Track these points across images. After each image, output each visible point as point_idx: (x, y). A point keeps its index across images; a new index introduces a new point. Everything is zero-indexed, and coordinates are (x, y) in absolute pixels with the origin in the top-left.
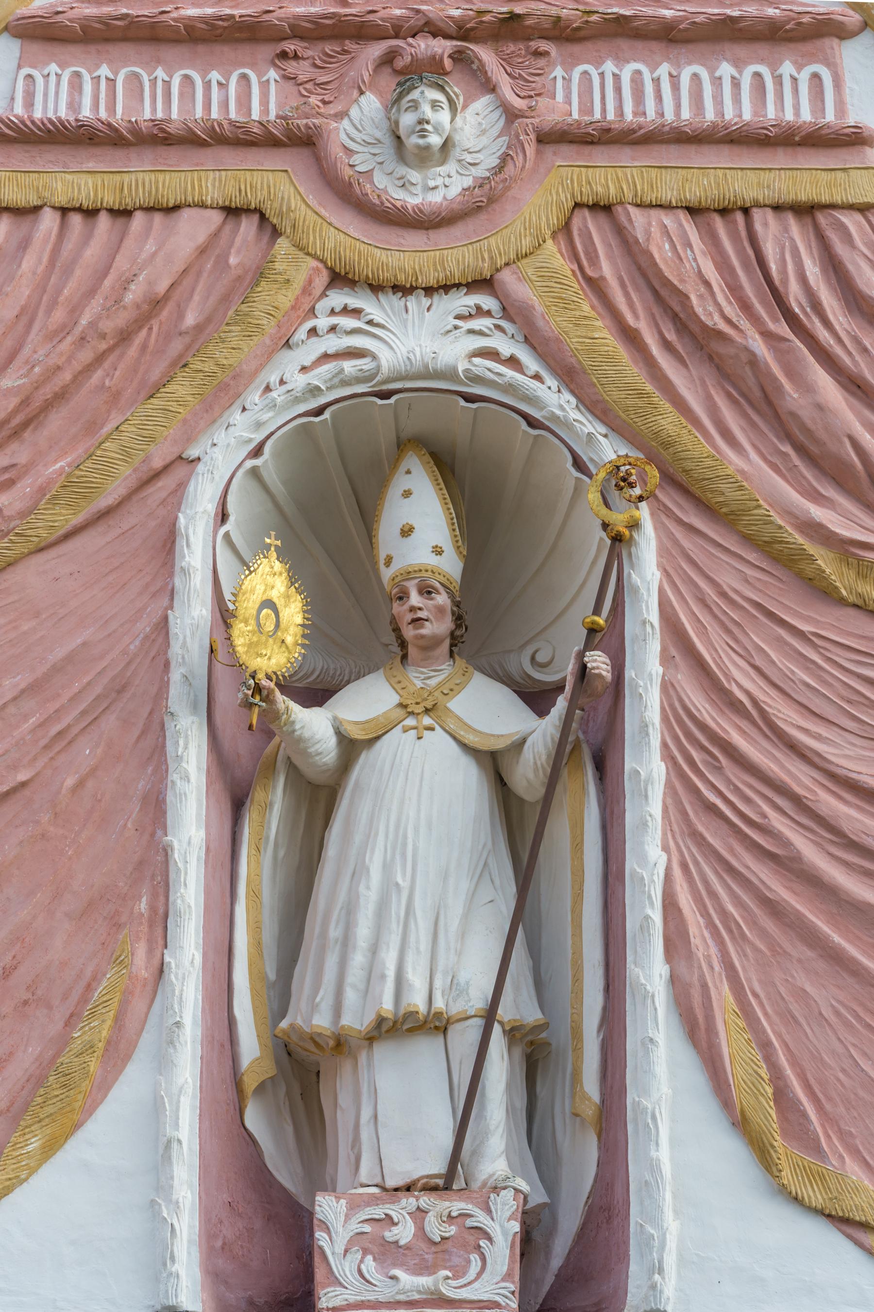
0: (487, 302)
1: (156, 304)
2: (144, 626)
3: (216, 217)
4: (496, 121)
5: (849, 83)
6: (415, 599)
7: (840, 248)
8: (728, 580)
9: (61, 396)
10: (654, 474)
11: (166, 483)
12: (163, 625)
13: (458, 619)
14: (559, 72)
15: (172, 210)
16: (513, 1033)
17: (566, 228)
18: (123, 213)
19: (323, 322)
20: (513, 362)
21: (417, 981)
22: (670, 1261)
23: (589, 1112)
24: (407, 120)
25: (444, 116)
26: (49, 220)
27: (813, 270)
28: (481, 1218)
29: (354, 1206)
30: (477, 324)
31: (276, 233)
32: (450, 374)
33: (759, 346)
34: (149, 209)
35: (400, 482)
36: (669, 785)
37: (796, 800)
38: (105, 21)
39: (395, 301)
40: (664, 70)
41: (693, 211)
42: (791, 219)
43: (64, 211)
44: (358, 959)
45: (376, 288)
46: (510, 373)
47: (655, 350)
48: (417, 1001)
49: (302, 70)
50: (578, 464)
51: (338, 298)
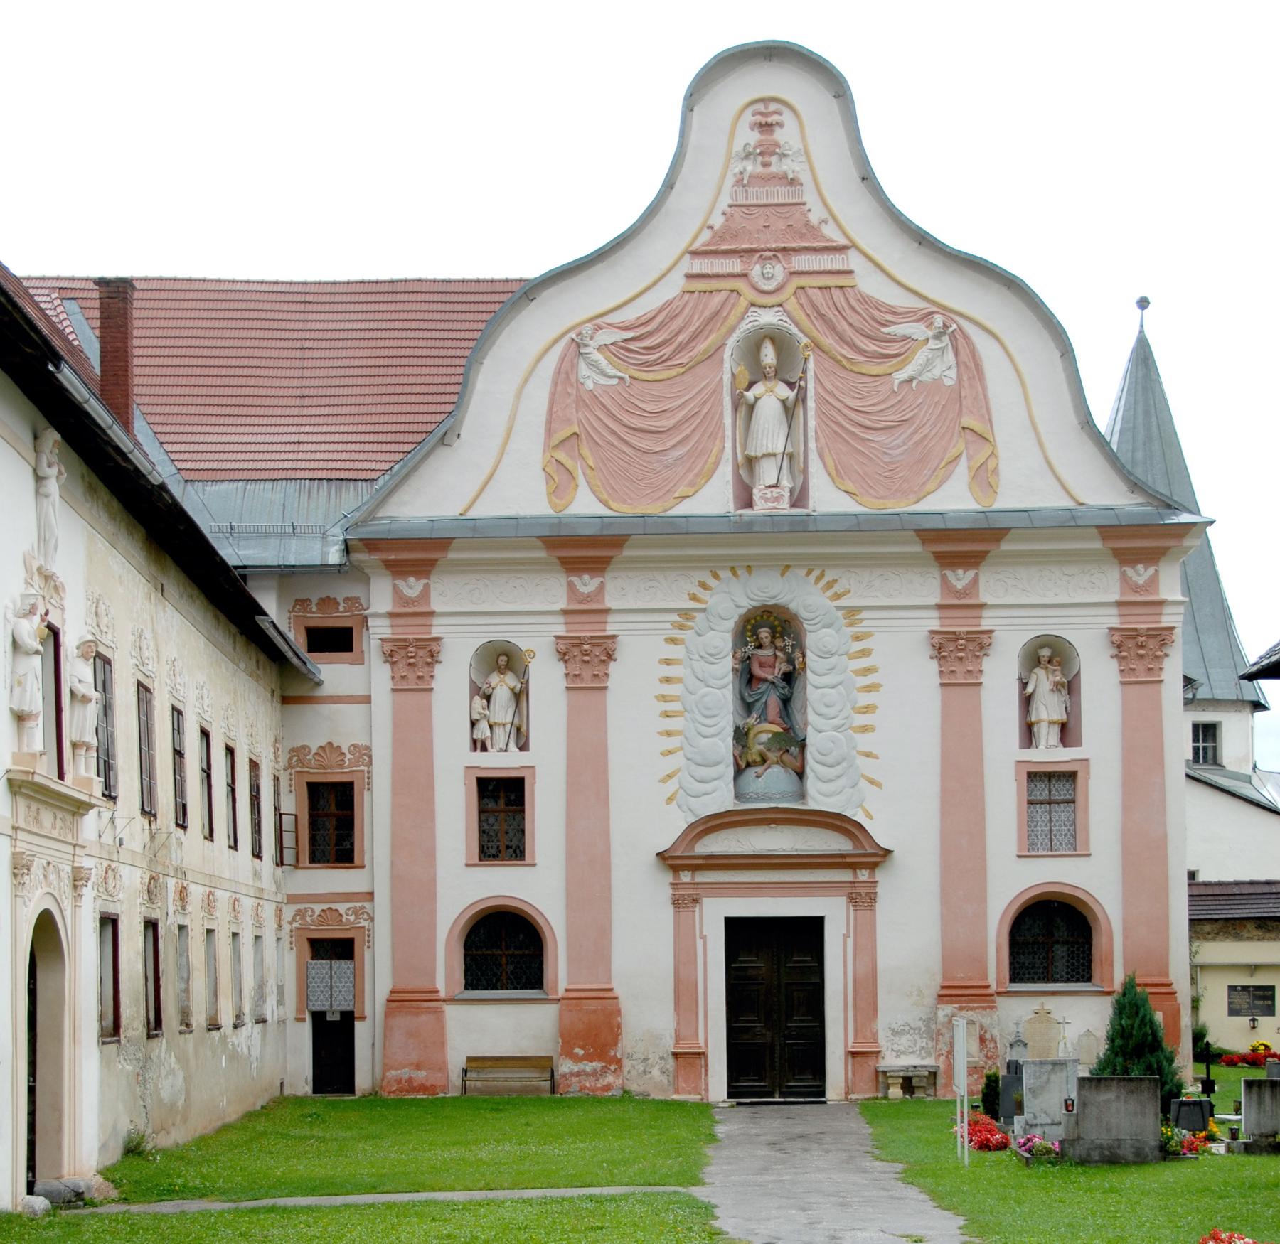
0: (780, 309)
3: (729, 292)
4: (782, 269)
6: (768, 369)
7: (848, 296)
8: (826, 366)
11: (719, 351)
12: (722, 378)
13: (776, 372)
14: (793, 258)
15: (720, 291)
17: (795, 292)
18: (711, 292)
19: (749, 314)
20: (786, 322)
21: (770, 445)
24: (765, 271)
25: (772, 271)
28: (782, 493)
30: (780, 314)
31: (740, 295)
32: (774, 325)
34: (716, 291)
36: (816, 410)
37: (839, 411)
39: (763, 309)
40: (814, 257)
41: (820, 288)
42: (838, 289)
43: (700, 292)
45: (760, 307)
46: (785, 324)
47: (813, 319)
48: (770, 451)
49: (744, 259)
51: (753, 309)
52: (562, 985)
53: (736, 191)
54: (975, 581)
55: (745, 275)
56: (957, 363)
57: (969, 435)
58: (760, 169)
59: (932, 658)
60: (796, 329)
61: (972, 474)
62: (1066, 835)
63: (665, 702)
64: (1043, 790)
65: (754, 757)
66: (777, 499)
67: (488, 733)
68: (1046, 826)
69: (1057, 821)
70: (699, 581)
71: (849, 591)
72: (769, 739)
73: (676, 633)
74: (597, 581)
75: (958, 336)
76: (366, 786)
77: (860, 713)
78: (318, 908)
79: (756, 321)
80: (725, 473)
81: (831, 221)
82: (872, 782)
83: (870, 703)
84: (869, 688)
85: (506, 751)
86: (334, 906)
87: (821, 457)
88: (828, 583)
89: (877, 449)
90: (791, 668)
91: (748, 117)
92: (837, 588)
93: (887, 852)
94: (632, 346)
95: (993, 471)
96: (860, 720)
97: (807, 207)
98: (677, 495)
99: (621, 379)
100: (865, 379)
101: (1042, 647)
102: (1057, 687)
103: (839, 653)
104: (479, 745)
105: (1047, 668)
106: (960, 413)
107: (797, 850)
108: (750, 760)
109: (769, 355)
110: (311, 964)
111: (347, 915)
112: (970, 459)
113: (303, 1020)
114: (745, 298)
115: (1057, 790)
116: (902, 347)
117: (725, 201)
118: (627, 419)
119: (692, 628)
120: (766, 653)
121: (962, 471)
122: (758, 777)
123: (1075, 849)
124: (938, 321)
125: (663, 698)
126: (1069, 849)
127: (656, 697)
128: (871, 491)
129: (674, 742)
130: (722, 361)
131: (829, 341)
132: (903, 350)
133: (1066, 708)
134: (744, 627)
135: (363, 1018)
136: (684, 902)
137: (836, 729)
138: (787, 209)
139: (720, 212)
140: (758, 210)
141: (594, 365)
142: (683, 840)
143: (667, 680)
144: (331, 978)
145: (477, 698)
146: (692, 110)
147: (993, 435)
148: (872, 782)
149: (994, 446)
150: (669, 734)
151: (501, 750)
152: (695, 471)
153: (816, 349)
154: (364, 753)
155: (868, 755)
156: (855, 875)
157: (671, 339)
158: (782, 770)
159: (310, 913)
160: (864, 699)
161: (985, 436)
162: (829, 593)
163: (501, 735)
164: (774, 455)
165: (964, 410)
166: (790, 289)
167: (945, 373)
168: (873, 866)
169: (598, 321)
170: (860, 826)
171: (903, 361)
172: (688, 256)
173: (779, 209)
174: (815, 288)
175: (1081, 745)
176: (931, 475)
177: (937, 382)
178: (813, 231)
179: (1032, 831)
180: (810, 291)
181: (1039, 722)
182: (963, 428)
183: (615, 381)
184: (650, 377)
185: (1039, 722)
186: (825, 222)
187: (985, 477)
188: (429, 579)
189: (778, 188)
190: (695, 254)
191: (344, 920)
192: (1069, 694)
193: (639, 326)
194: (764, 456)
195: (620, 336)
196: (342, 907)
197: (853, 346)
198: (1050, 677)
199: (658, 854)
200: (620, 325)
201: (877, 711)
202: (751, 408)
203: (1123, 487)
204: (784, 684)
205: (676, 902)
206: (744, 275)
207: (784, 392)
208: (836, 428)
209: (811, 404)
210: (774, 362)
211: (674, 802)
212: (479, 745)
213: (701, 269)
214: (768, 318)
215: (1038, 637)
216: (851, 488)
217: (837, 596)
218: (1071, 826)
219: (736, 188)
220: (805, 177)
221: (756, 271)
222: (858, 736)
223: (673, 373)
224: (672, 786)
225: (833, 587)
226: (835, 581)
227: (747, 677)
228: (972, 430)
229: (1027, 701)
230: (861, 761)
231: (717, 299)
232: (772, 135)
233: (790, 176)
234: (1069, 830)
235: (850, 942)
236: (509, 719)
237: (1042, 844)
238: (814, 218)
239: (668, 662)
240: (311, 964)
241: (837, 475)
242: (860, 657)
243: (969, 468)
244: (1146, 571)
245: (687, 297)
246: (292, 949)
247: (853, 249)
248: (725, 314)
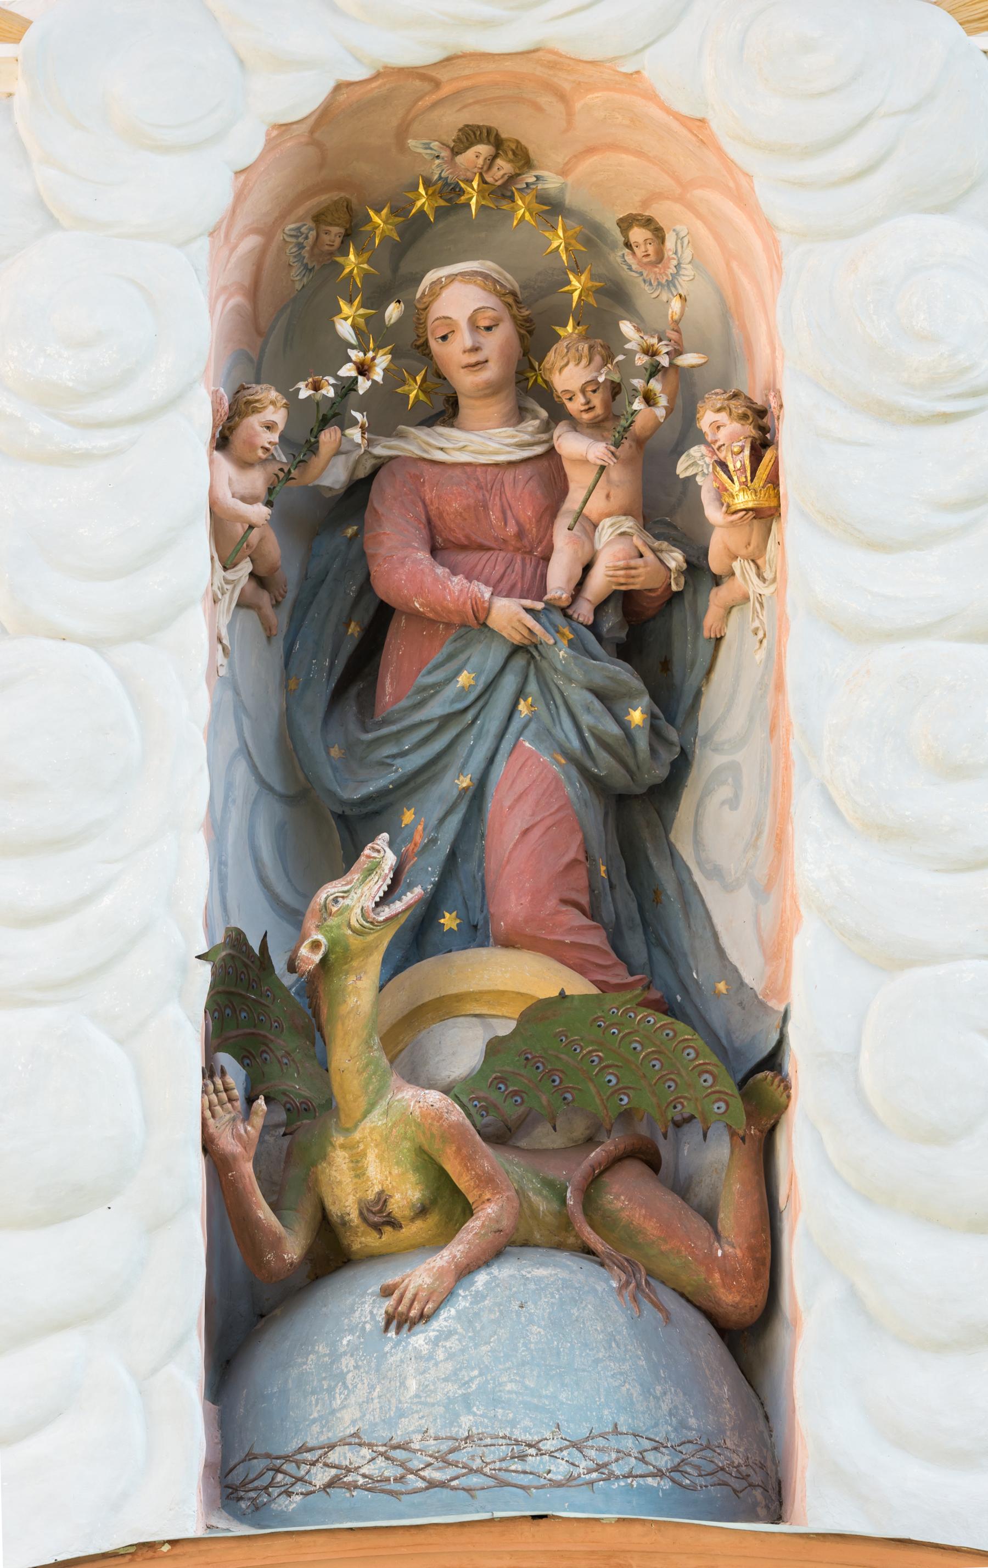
72: (494, 1047)
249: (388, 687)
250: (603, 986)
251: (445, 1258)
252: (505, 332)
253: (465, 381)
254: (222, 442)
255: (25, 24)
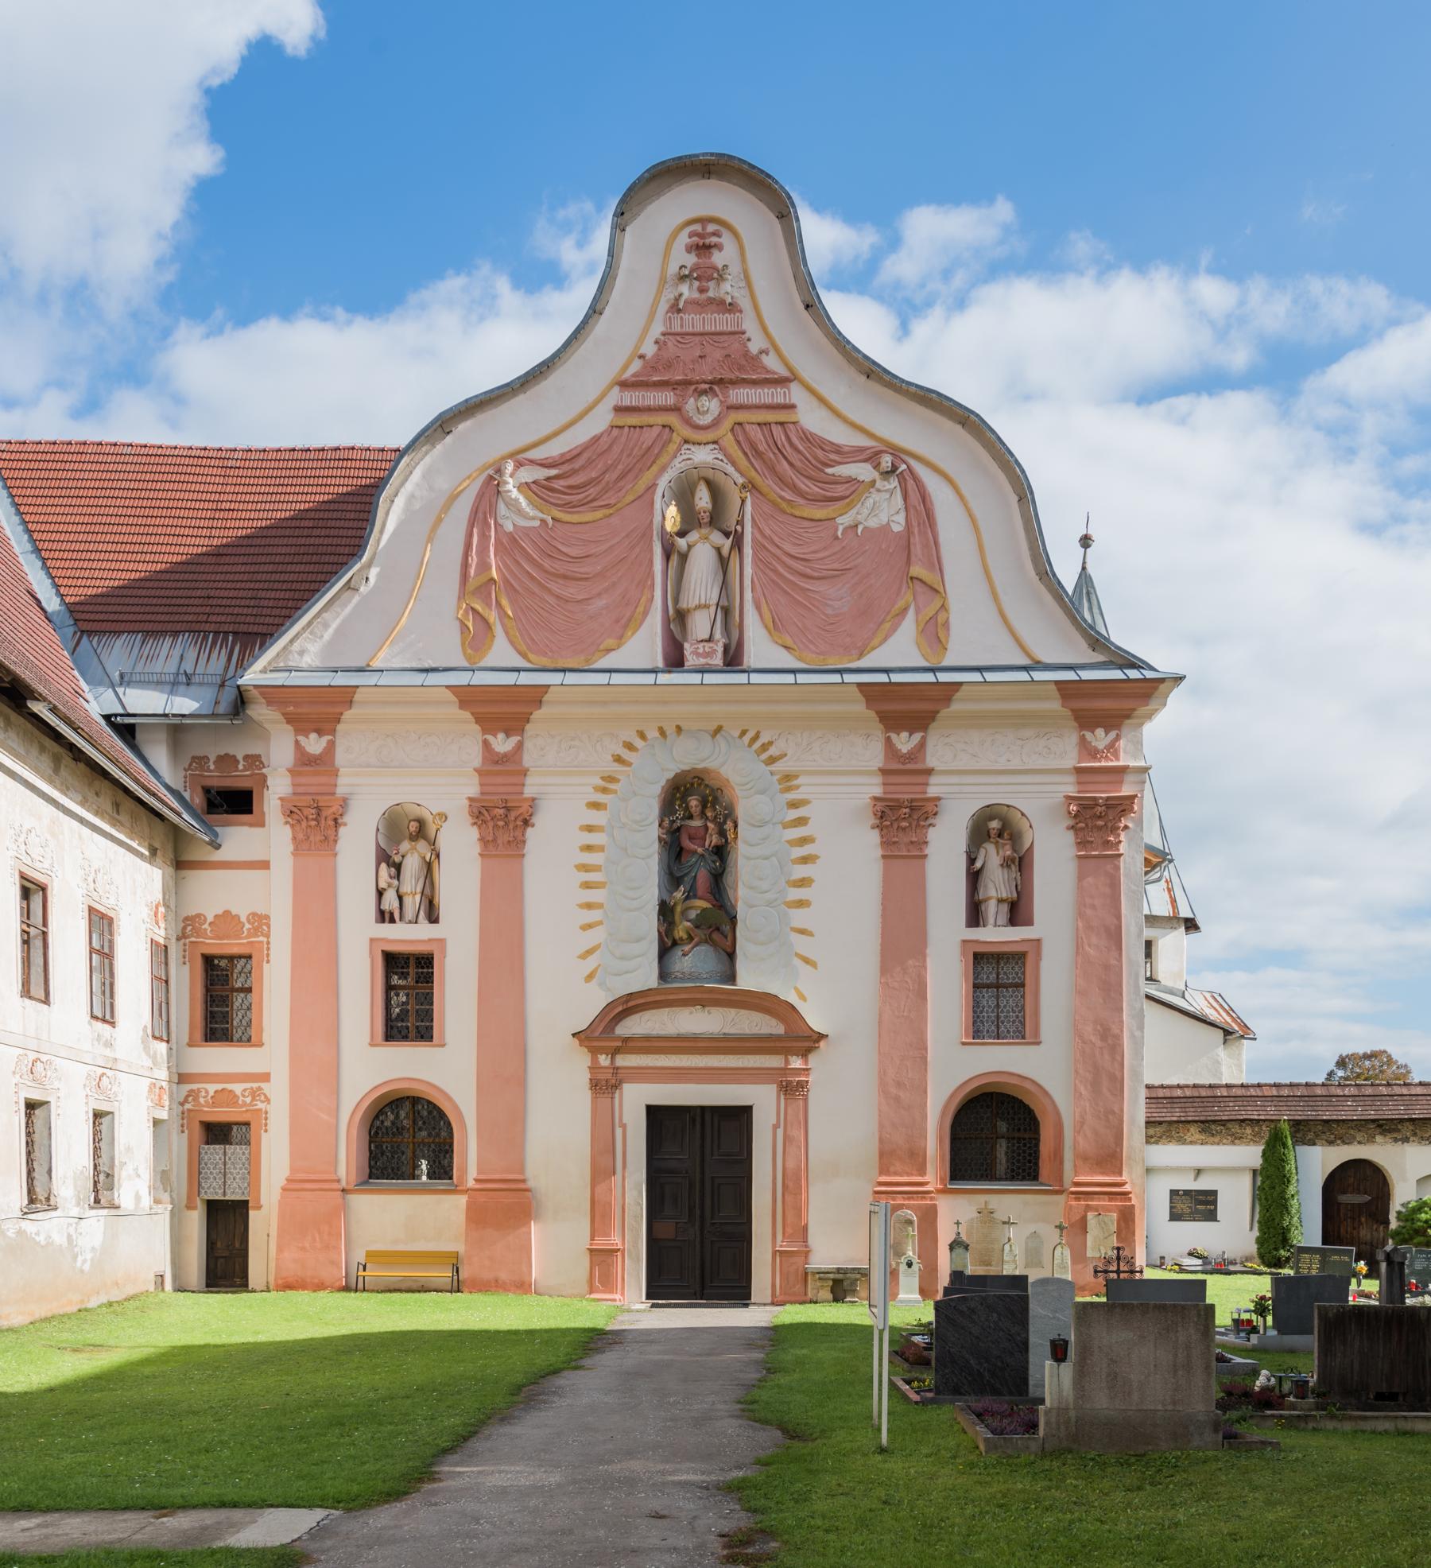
0: (717, 447)
1: (649, 448)
2: (648, 521)
4: (719, 404)
5: (792, 393)
9: (630, 470)
10: (750, 486)
11: (652, 489)
12: (652, 521)
13: (711, 518)
14: (731, 392)
15: (651, 426)
16: (722, 608)
18: (641, 427)
19: (683, 452)
20: (722, 460)
22: (752, 656)
23: (737, 624)
24: (699, 404)
26: (626, 429)
27: (783, 438)
28: (715, 647)
29: (692, 645)
30: (716, 451)
32: (709, 463)
33: (771, 455)
35: (699, 488)
37: (778, 558)
38: (637, 381)
39: (697, 446)
41: (759, 424)
42: (779, 426)
43: (630, 427)
44: (691, 593)
45: (694, 444)
48: (703, 602)
49: (678, 392)
50: (735, 483)
51: (686, 446)
52: (472, 1173)
53: (670, 317)
54: (922, 745)
55: (676, 409)
56: (906, 508)
57: (918, 586)
58: (696, 295)
59: (873, 828)
60: (733, 469)
61: (920, 629)
62: (1014, 1022)
63: (586, 871)
64: (991, 973)
65: (681, 934)
66: (706, 655)
67: (396, 904)
68: (993, 1012)
69: (1005, 1007)
70: (624, 742)
71: (786, 755)
72: (697, 915)
73: (601, 798)
74: (514, 740)
75: (907, 478)
76: (266, 959)
77: (794, 886)
78: (212, 1088)
79: (690, 459)
80: (654, 623)
81: (772, 353)
82: (807, 961)
83: (806, 876)
84: (805, 860)
85: (416, 923)
86: (229, 1086)
87: (758, 607)
88: (763, 745)
89: (818, 600)
90: (723, 840)
91: (684, 239)
92: (773, 751)
93: (822, 1036)
94: (558, 485)
95: (943, 625)
96: (795, 894)
97: (747, 335)
98: (602, 647)
99: (543, 521)
100: (806, 524)
101: (992, 818)
102: (1007, 863)
103: (774, 820)
104: (384, 917)
105: (998, 842)
106: (908, 562)
107: (725, 1034)
108: (677, 937)
109: (703, 500)
110: (204, 1148)
111: (244, 1096)
112: (917, 612)
113: (195, 1208)
114: (678, 434)
115: (1005, 973)
116: (847, 489)
117: (657, 329)
118: (547, 564)
119: (615, 792)
120: (697, 823)
121: (908, 627)
122: (684, 955)
123: (1023, 1037)
124: (886, 461)
125: (584, 868)
126: (1017, 1038)
127: (576, 866)
128: (811, 646)
129: (595, 915)
130: (652, 503)
131: (767, 483)
132: (848, 493)
133: (1016, 886)
134: (673, 795)
135: (259, 1207)
136: (605, 1086)
137: (769, 904)
138: (725, 337)
139: (654, 340)
140: (694, 338)
141: (513, 505)
142: (601, 1021)
143: (588, 848)
144: (225, 1164)
145: (383, 866)
146: (624, 230)
147: (944, 586)
148: (807, 961)
149: (945, 599)
150: (589, 906)
151: (410, 922)
152: (623, 621)
153: (754, 491)
154: (261, 922)
155: (802, 932)
156: (787, 1062)
157: (597, 478)
158: (712, 949)
159: (203, 1094)
160: (800, 871)
161: (935, 586)
162: (764, 756)
163: (412, 903)
164: (707, 606)
165: (913, 558)
166: (727, 424)
167: (893, 518)
168: (805, 1053)
169: (520, 457)
170: (793, 1007)
171: (848, 504)
172: (617, 389)
173: (716, 338)
174: (753, 423)
175: (1032, 925)
176: (877, 630)
177: (886, 528)
178: (754, 361)
179: (978, 1017)
180: (747, 427)
181: (989, 898)
182: (912, 578)
183: (537, 523)
184: (575, 518)
185: (989, 898)
186: (765, 352)
187: (934, 633)
188: (333, 732)
189: (716, 315)
190: (624, 385)
191: (240, 1102)
192: (1020, 871)
193: (563, 463)
194: (699, 607)
195: (541, 474)
196: (237, 1088)
197: (794, 489)
198: (1001, 852)
199: (574, 1035)
200: (544, 462)
201: (814, 884)
202: (684, 557)
203: (1083, 644)
204: (715, 858)
205: (596, 1085)
206: (676, 409)
207: (717, 538)
208: (774, 578)
209: (748, 550)
210: (709, 506)
211: (595, 980)
212: (384, 917)
213: (631, 402)
214: (703, 456)
215: (988, 806)
216: (789, 642)
217: (772, 760)
218: (1020, 1012)
219: (669, 314)
220: (744, 303)
221: (690, 404)
222: (793, 912)
223: (599, 514)
224: (591, 963)
225: (768, 749)
226: (771, 743)
227: (674, 849)
228: (921, 580)
229: (974, 877)
230: (795, 938)
231: (649, 436)
232: (710, 258)
233: (729, 300)
234: (1017, 1017)
235: (780, 1132)
236: (419, 889)
237: (988, 1031)
238: (754, 348)
239: (590, 829)
240: (204, 1148)
241: (775, 627)
242: (795, 826)
243: (917, 621)
244: (1106, 735)
245: (615, 432)
246: (183, 1132)
247: (795, 382)
248: (656, 452)
249: (683, 859)
250: (714, 906)
251: (690, 946)
252: (700, 807)
253: (695, 814)
254: (660, 825)
255: (632, 764)
